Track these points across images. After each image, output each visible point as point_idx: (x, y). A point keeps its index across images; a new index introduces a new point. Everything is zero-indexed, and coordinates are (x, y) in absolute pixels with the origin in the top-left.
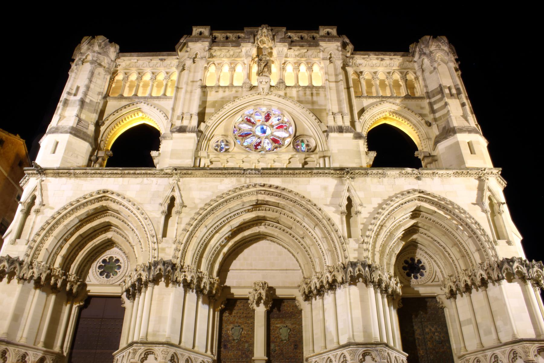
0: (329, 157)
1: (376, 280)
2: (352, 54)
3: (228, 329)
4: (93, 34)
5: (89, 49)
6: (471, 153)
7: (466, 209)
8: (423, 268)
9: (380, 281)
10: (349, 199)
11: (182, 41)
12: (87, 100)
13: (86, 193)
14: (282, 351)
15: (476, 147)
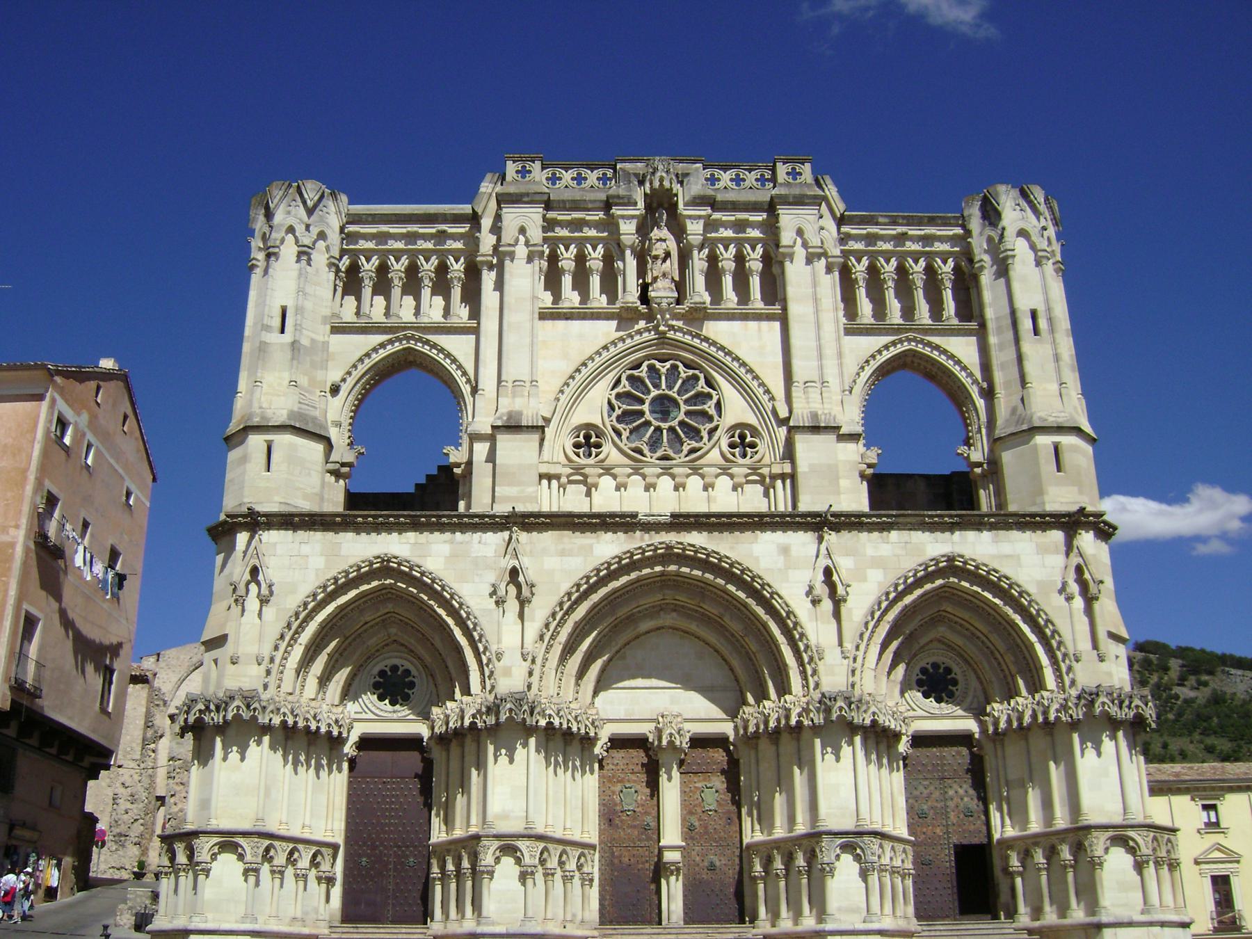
0: (793, 477)
1: (868, 722)
2: (841, 221)
3: (614, 793)
4: (293, 175)
5: (289, 213)
6: (1059, 470)
7: (1031, 589)
8: (955, 682)
9: (874, 722)
10: (828, 572)
11: (482, 190)
12: (305, 342)
13: (352, 561)
14: (706, 828)
15: (1066, 457)
